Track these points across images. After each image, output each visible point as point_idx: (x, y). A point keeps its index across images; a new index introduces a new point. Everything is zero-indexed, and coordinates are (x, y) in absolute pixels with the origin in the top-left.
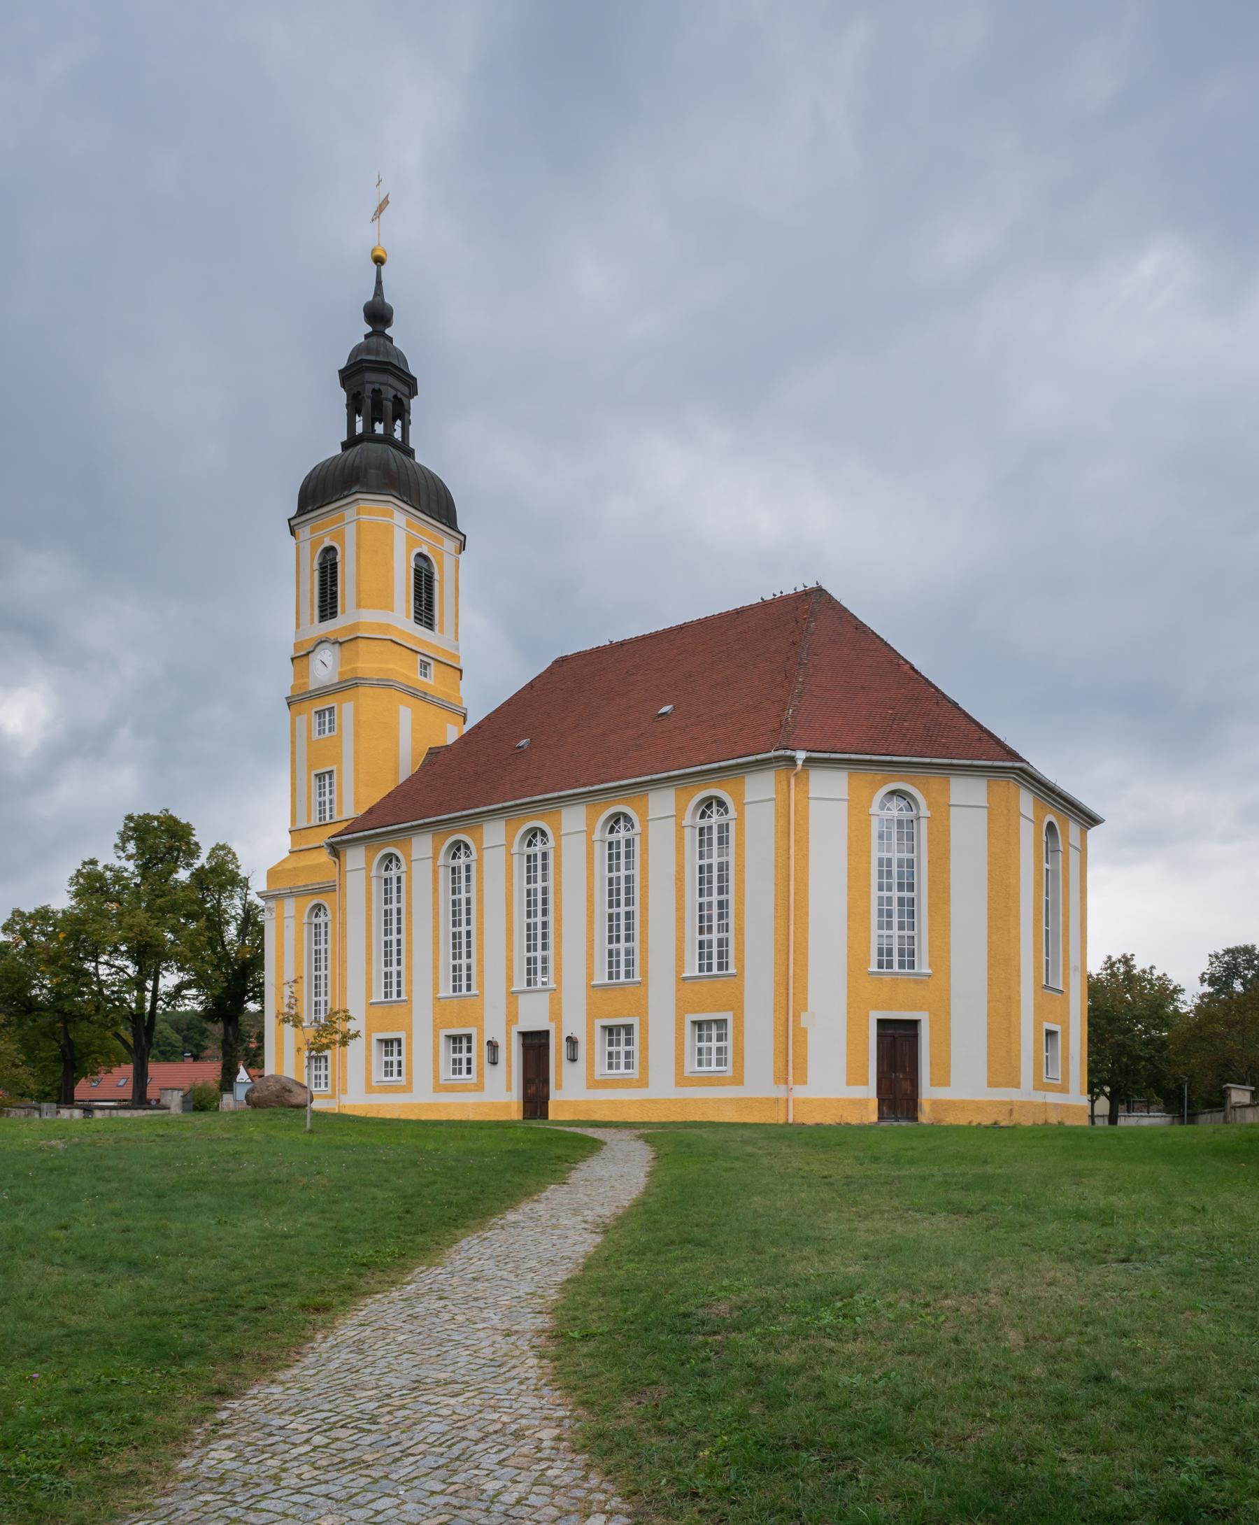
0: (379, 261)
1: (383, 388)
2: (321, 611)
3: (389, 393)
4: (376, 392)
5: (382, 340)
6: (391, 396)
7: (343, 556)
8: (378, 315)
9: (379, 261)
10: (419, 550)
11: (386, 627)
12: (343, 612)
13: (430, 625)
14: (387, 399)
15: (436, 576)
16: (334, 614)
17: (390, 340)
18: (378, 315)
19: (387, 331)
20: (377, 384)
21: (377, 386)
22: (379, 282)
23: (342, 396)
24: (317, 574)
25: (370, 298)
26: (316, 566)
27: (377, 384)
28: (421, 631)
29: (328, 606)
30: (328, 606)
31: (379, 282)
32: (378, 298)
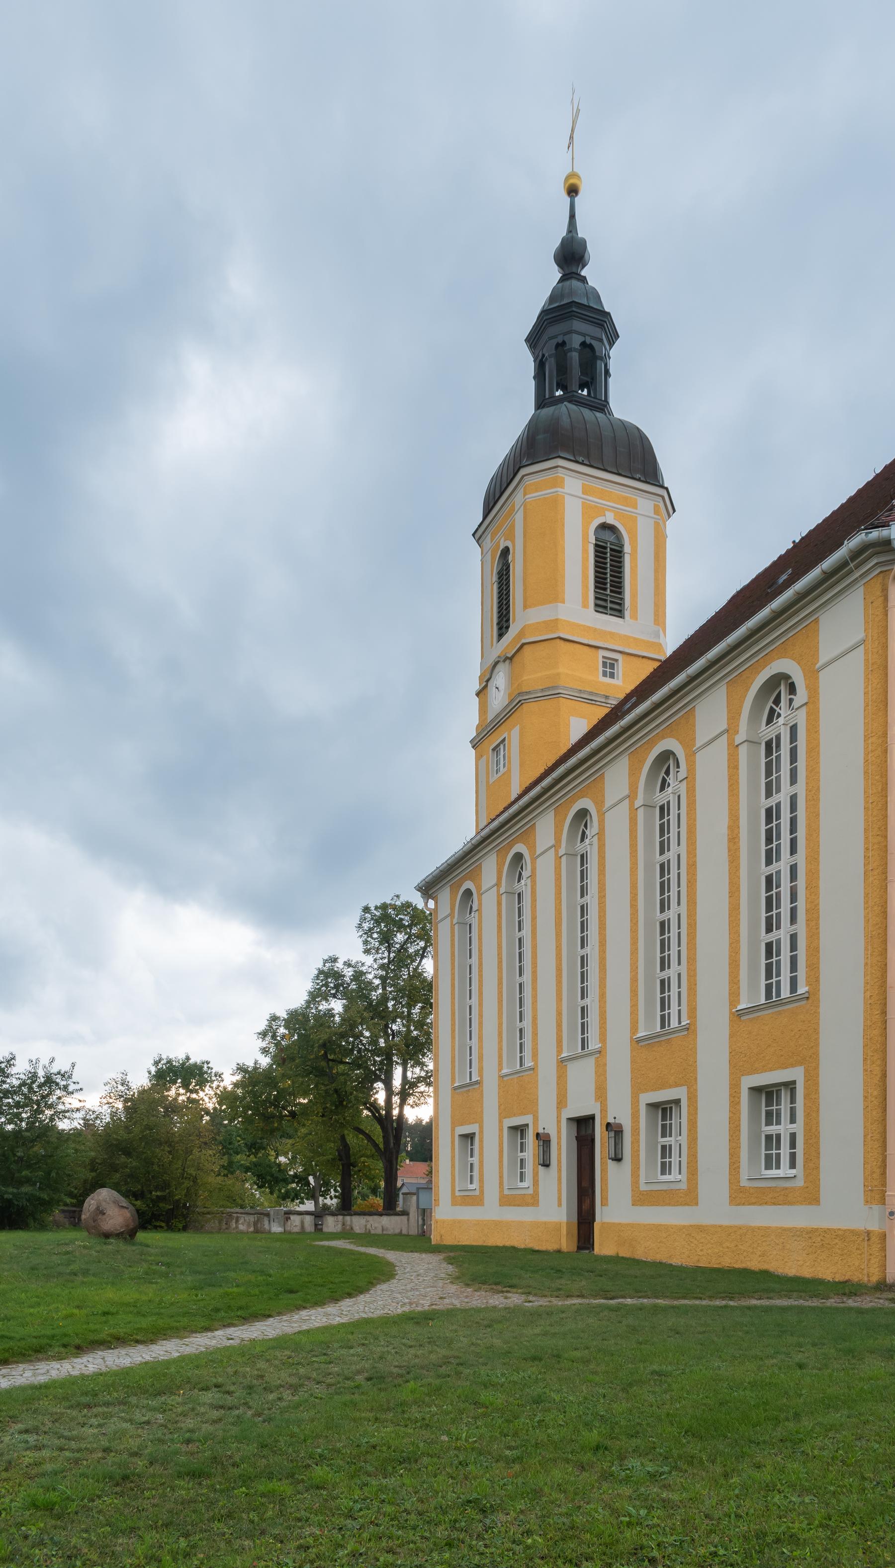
0: (573, 191)
5: (575, 283)
8: (571, 256)
9: (573, 191)
13: (619, 612)
15: (627, 549)
17: (584, 280)
18: (571, 256)
19: (583, 273)
20: (571, 342)
22: (572, 216)
27: (571, 342)
28: (608, 622)
31: (572, 216)
32: (570, 235)
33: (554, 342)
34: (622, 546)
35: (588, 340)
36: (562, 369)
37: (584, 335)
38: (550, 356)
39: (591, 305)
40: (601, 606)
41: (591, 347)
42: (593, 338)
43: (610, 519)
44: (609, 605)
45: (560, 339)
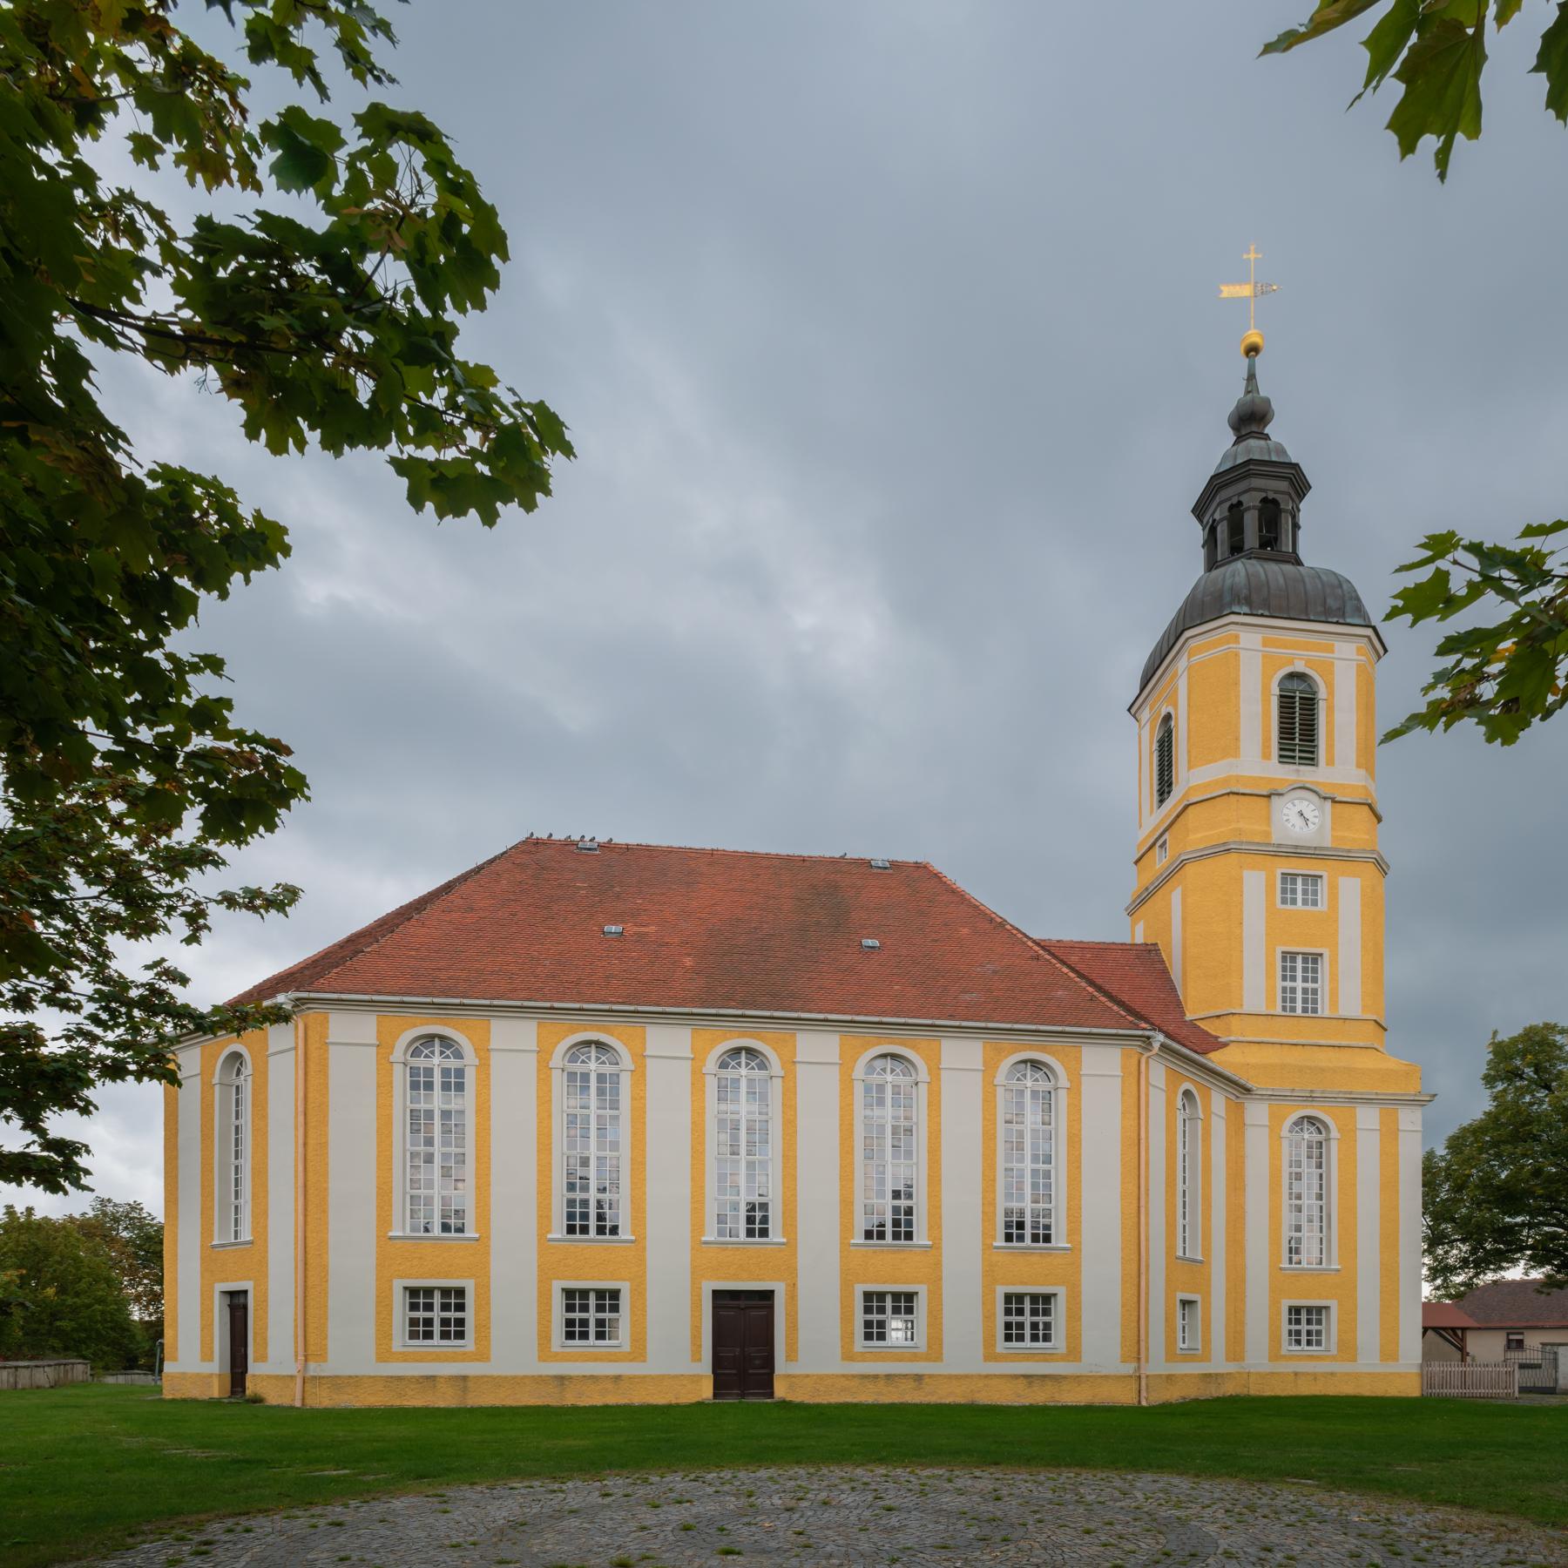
8: (1251, 420)
15: (1322, 693)
17: (1267, 437)
18: (1251, 420)
22: (1251, 377)
23: (1196, 533)
26: (1155, 746)
31: (1251, 377)
33: (1228, 504)
34: (1315, 693)
35: (1271, 496)
36: (1236, 529)
37: (1265, 491)
38: (1222, 520)
39: (1274, 459)
40: (1286, 755)
41: (1275, 502)
42: (1276, 492)
43: (1299, 667)
44: (1297, 754)
45: (1234, 501)
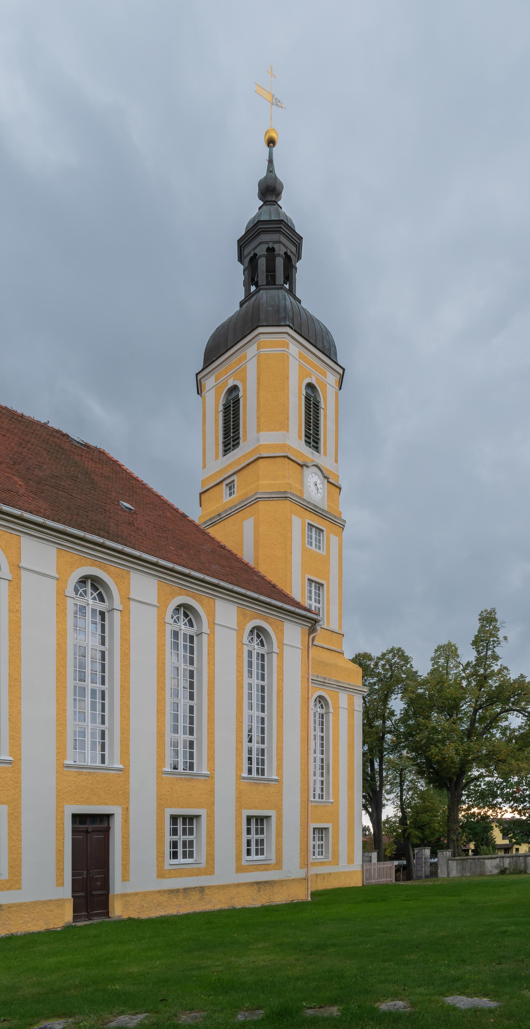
1: (276, 246)
2: (225, 446)
3: (280, 250)
4: (271, 250)
6: (282, 253)
7: (245, 391)
10: (307, 380)
11: (283, 446)
12: (245, 439)
14: (279, 255)
16: (236, 445)
21: (271, 245)
22: (271, 161)
24: (221, 415)
25: (264, 174)
26: (221, 408)
29: (231, 437)
30: (231, 437)
31: (271, 161)
